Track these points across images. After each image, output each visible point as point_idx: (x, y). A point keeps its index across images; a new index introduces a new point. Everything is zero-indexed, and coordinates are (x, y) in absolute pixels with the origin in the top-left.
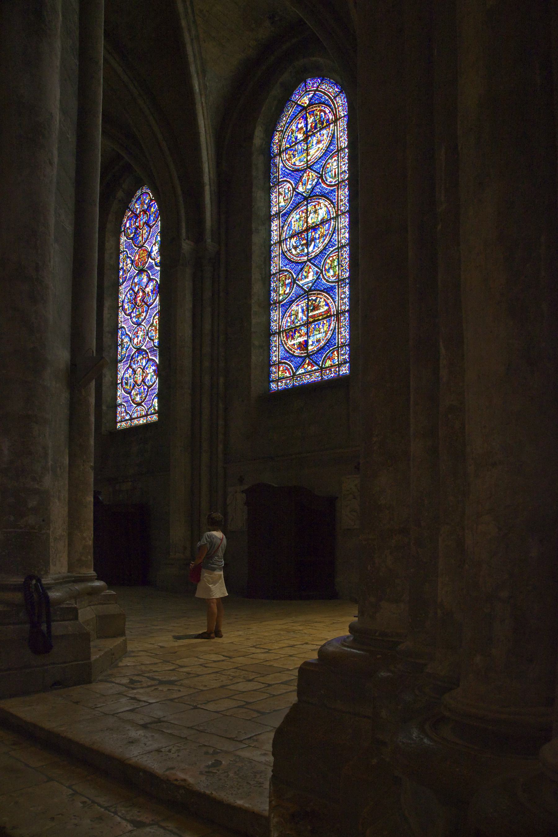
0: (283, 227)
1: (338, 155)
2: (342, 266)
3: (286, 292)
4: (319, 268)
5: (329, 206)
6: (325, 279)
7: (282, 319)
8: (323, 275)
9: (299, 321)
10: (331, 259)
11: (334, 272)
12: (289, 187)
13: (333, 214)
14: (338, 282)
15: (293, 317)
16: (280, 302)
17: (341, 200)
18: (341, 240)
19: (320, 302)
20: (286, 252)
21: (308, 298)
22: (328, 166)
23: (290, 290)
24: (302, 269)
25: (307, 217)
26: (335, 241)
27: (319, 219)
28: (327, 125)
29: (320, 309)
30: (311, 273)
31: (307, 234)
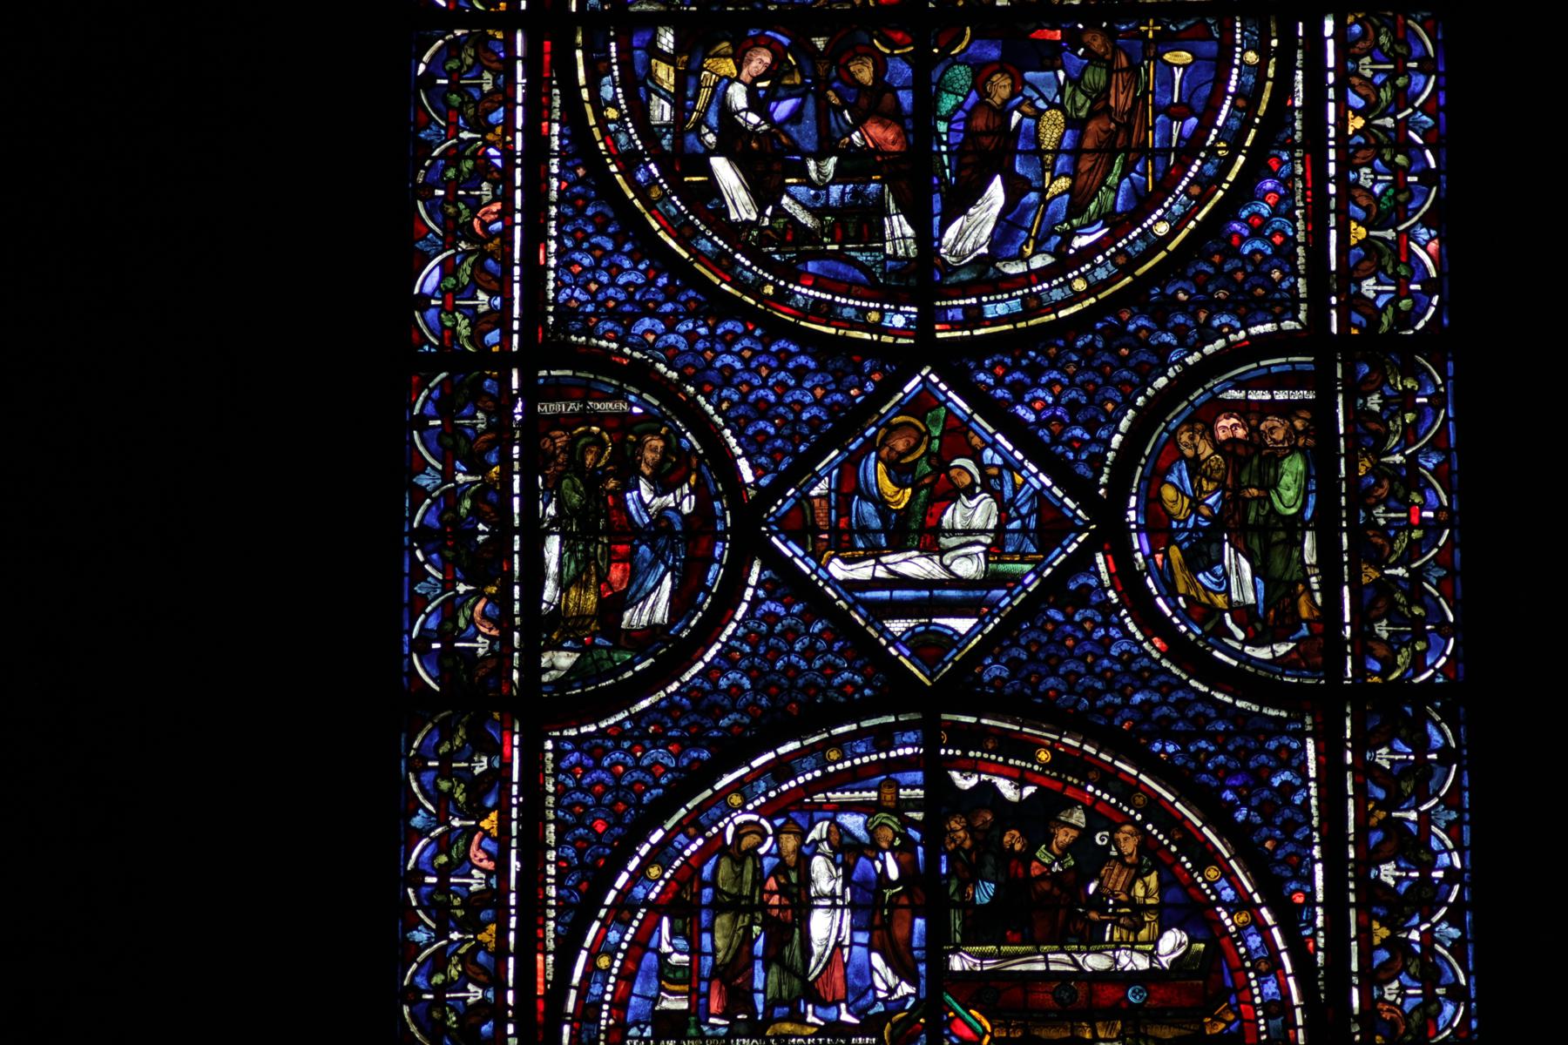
2: (1370, 549)
3: (634, 618)
4: (1081, 489)
6: (1153, 623)
7: (577, 916)
8: (1127, 577)
9: (812, 994)
10: (1227, 426)
11: (1280, 587)
14: (1322, 707)
15: (719, 938)
16: (543, 709)
18: (1350, 275)
19: (1089, 858)
21: (935, 771)
23: (681, 604)
24: (845, 423)
26: (1285, 253)
29: (1093, 940)
30: (979, 512)
31: (922, 65)
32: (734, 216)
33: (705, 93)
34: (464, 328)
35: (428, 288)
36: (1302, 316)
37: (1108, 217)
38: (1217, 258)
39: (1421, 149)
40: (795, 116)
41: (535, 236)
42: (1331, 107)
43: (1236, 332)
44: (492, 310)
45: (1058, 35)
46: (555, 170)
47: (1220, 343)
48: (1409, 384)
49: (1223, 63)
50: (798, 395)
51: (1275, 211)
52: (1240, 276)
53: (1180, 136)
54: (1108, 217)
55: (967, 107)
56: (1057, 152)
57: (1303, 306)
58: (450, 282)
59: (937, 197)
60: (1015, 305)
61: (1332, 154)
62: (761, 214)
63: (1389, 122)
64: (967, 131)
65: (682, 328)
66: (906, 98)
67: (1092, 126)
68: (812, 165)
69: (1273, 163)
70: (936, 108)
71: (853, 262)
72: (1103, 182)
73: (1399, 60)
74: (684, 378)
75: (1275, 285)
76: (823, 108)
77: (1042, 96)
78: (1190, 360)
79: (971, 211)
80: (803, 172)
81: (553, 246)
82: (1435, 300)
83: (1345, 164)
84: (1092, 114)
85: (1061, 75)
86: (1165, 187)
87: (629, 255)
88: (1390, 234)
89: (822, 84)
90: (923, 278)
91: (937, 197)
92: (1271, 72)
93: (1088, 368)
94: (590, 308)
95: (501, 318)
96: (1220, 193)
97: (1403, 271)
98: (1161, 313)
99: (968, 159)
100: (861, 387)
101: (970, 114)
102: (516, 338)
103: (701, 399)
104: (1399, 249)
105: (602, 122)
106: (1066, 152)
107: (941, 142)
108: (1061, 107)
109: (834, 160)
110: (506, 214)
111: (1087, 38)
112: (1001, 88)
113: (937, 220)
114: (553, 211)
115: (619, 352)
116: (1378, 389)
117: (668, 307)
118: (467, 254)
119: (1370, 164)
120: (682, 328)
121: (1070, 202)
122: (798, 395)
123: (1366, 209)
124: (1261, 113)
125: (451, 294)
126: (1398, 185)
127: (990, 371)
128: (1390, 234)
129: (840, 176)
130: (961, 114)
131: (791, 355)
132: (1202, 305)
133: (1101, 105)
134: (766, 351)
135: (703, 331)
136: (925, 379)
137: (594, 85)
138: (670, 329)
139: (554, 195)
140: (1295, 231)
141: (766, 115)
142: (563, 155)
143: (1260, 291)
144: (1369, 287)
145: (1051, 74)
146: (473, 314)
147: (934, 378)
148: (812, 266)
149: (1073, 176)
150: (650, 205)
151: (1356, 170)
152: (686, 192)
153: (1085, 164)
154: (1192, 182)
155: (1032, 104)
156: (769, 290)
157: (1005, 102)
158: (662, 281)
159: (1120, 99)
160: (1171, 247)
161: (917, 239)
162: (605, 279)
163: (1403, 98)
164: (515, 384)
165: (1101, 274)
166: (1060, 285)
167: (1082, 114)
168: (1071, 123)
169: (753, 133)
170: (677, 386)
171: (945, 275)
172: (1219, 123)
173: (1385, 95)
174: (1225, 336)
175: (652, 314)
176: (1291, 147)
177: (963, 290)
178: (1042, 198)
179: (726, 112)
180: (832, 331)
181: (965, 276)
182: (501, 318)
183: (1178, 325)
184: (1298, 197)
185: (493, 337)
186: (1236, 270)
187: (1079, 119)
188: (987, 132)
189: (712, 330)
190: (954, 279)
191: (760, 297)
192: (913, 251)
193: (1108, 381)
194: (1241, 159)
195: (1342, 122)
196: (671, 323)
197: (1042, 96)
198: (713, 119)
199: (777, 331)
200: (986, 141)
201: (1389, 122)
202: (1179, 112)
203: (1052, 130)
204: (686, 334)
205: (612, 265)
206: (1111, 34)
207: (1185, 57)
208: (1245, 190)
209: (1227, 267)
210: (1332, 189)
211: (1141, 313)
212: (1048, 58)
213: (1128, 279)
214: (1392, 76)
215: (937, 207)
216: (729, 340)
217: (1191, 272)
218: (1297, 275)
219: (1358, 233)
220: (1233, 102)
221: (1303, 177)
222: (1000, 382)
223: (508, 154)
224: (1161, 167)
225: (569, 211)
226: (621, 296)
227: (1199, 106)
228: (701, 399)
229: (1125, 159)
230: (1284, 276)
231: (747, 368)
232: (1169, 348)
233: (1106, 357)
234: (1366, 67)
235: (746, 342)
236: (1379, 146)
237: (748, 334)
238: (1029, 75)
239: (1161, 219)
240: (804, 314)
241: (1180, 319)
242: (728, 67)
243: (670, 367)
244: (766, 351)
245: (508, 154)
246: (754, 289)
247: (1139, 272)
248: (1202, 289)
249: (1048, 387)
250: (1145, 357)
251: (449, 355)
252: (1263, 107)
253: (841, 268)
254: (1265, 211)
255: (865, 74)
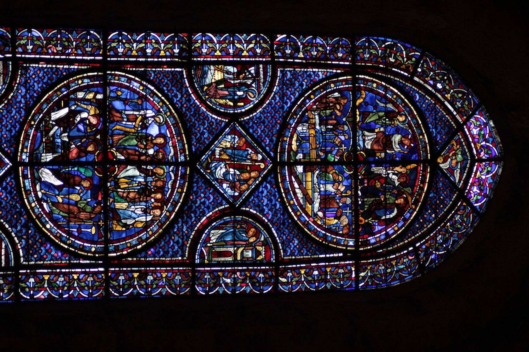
0: (143, 76)
1: (269, 263)
5: (143, 235)
12: (246, 101)
13: (116, 250)
17: (143, 276)
18: (35, 275)
20: (67, 86)
22: (252, 231)
25: (138, 165)
26: (41, 258)
27: (121, 205)
28: (358, 226)
31: (92, 164)
32: (52, 114)
33: (85, 106)
34: (23, 42)
35: (33, 33)
36: (24, 263)
37: (51, 212)
38: (40, 240)
39: (68, 294)
40: (79, 130)
41: (47, 61)
42: (80, 270)
43: (20, 245)
44: (27, 50)
45: (100, 199)
46: (65, 67)
47: (17, 241)
48: (6, 291)
49: (92, 242)
50: (4, 130)
51: (52, 256)
52: (35, 247)
53: (72, 231)
54: (51, 212)
55: (81, 175)
56: (69, 199)
57: (27, 263)
58: (35, 39)
59: (57, 167)
60: (28, 188)
61: (67, 270)
62: (53, 121)
63: (76, 285)
64: (75, 175)
65: (23, 100)
66: (84, 159)
67: (75, 208)
68: (66, 134)
69: (65, 255)
70: (81, 167)
71: (40, 145)
72: (61, 211)
73: (92, 288)
74: (9, 100)
75: (33, 256)
76: (81, 138)
77: (84, 195)
78: (13, 234)
79: (53, 176)
80: (64, 132)
81: (45, 66)
82: (28, 297)
83: (65, 274)
84: (79, 208)
85: (89, 200)
86: (59, 227)
87: (42, 86)
88: (46, 286)
89: (87, 137)
90: (36, 163)
91: (57, 167)
92: (89, 254)
93: (11, 207)
94: (28, 75)
95: (25, 52)
96: (57, 241)
97: (36, 289)
98: (26, 226)
99: (67, 175)
100: (6, 147)
101: (79, 176)
102: (20, 56)
103: (3, 105)
104: (41, 288)
105: (78, 79)
106: (69, 201)
107: (72, 168)
108: (81, 200)
109: (67, 140)
110: (53, 54)
111: (99, 207)
112: (86, 184)
113: (51, 167)
114: (54, 66)
115: (16, 83)
116: (5, 283)
117: (28, 96)
118: (43, 43)
119: (65, 280)
120: (23, 100)
121: (55, 202)
122: (4, 130)
123: (53, 280)
124: (79, 252)
125: (32, 39)
126: (59, 288)
127: (10, 181)
128: (46, 286)
129: (63, 142)
130: (79, 174)
131: (15, 128)
132: (27, 236)
133: (81, 210)
134: (16, 122)
135: (22, 105)
136: (8, 164)
137: (88, 77)
138: (22, 97)
139: (58, 66)
140: (47, 261)
141: (79, 123)
142: (69, 69)
143: (31, 252)
144: (32, 280)
145: (90, 197)
146: (26, 45)
147: (9, 166)
148: (39, 134)
149: (62, 203)
150: (56, 92)
151: (63, 277)
152: (59, 101)
153: (65, 206)
154: (61, 234)
155: (82, 192)
156: (33, 123)
157: (82, 185)
158: (35, 95)
159: (83, 215)
160: (43, 229)
161: (46, 162)
162: (36, 79)
163: (82, 289)
164: (8, 55)
165: (36, 210)
166: (33, 200)
167: (79, 205)
168: (77, 203)
169: (74, 119)
170: (7, 99)
171: (36, 169)
172: (76, 241)
173: (83, 284)
174: (19, 243)
175: (26, 92)
176: (69, 260)
177: (32, 174)
178: (56, 195)
179: (80, 112)
180: (22, 139)
181: (36, 174)
182: (25, 52)
183: (22, 230)
184: (56, 262)
185: (20, 50)
186: (37, 246)
187: (77, 204)
188: (74, 181)
189: (22, 108)
190: (35, 171)
191: (30, 121)
192: (43, 161)
193: (7, 212)
194: (66, 247)
195: (76, 273)
196: (24, 97)
197: (84, 195)
198: (78, 108)
199: (22, 125)
200: (72, 180)
201: (76, 285)
202: (79, 231)
203: (75, 197)
204: (21, 101)
205: (40, 82)
206: (100, 213)
207: (94, 232)
208: (58, 248)
209: (38, 243)
210: (58, 270)
211: (26, 221)
212: (94, 197)
213: (35, 217)
214: (88, 286)
215: (55, 167)
216: (19, 112)
217: (37, 234)
218: (35, 261)
219: (46, 277)
220: (81, 245)
221: (61, 263)
222: (7, 184)
223: (69, 54)
224: (64, 226)
225: (54, 70)
226: (31, 84)
227: (81, 236)
228: (3, 105)
229: (67, 217)
230: (35, 258)
231: (11, 117)
232: (16, 228)
233: (14, 212)
234: (90, 279)
235: (19, 117)
236: (69, 283)
237: (21, 117)
238: (89, 191)
239: (51, 226)
240: (26, 132)
241: (24, 231)
242: (92, 112)
243: (12, 97)
244: (16, 122)
245: (69, 54)
246: (33, 119)
247: (37, 220)
248: (32, 237)
249: (6, 196)
250: (14, 222)
251: (15, 38)
252: (80, 252)
253: (39, 142)
254: (53, 253)
255: (90, 148)
